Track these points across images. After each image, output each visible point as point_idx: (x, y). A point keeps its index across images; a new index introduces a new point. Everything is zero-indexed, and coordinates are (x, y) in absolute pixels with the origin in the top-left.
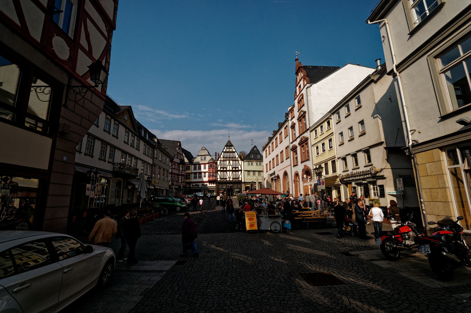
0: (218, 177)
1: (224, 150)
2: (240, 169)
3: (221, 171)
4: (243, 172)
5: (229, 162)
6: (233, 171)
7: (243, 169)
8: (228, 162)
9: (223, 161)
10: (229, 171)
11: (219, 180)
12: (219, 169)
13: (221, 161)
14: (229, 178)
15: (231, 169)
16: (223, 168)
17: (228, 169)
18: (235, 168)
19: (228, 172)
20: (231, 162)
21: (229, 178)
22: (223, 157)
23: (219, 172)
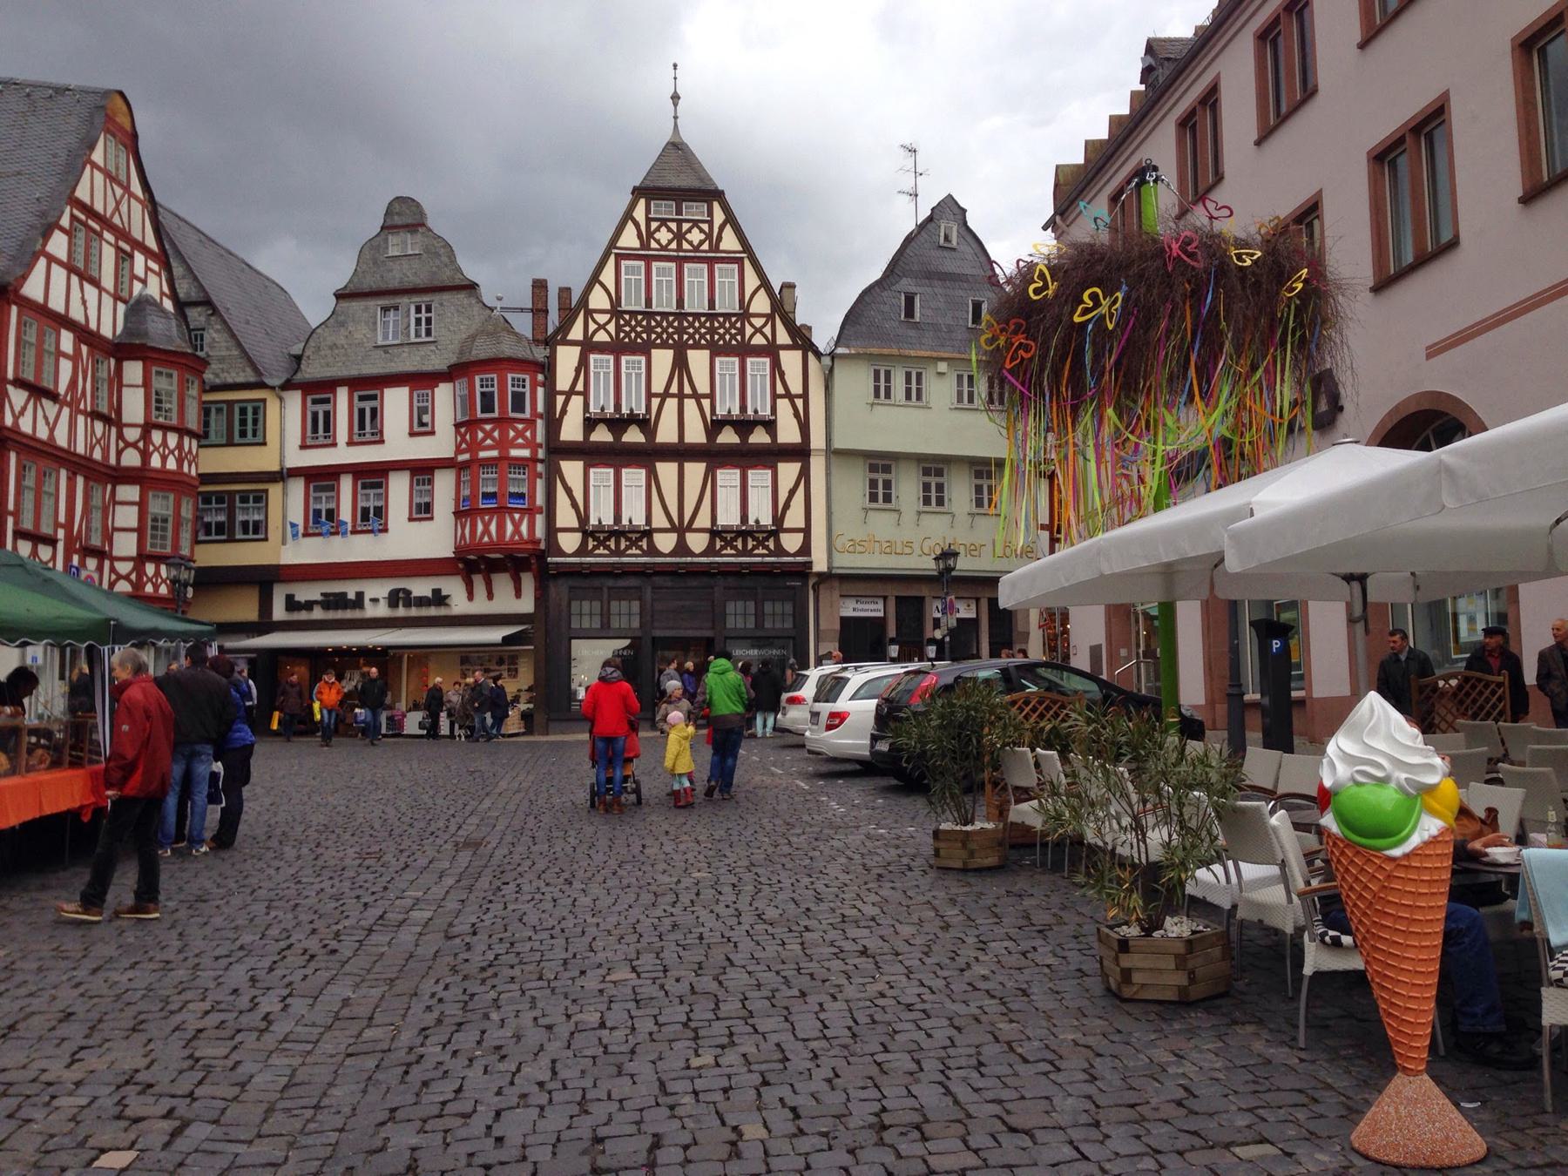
0: (565, 516)
2: (788, 433)
3: (589, 454)
4: (817, 465)
5: (681, 364)
6: (714, 456)
7: (817, 441)
8: (663, 359)
9: (617, 348)
10: (681, 453)
11: (569, 542)
12: (571, 431)
13: (588, 346)
14: (681, 529)
15: (696, 434)
16: (618, 424)
17: (666, 433)
18: (744, 426)
19: (667, 471)
20: (698, 360)
21: (681, 529)
22: (615, 312)
23: (572, 470)
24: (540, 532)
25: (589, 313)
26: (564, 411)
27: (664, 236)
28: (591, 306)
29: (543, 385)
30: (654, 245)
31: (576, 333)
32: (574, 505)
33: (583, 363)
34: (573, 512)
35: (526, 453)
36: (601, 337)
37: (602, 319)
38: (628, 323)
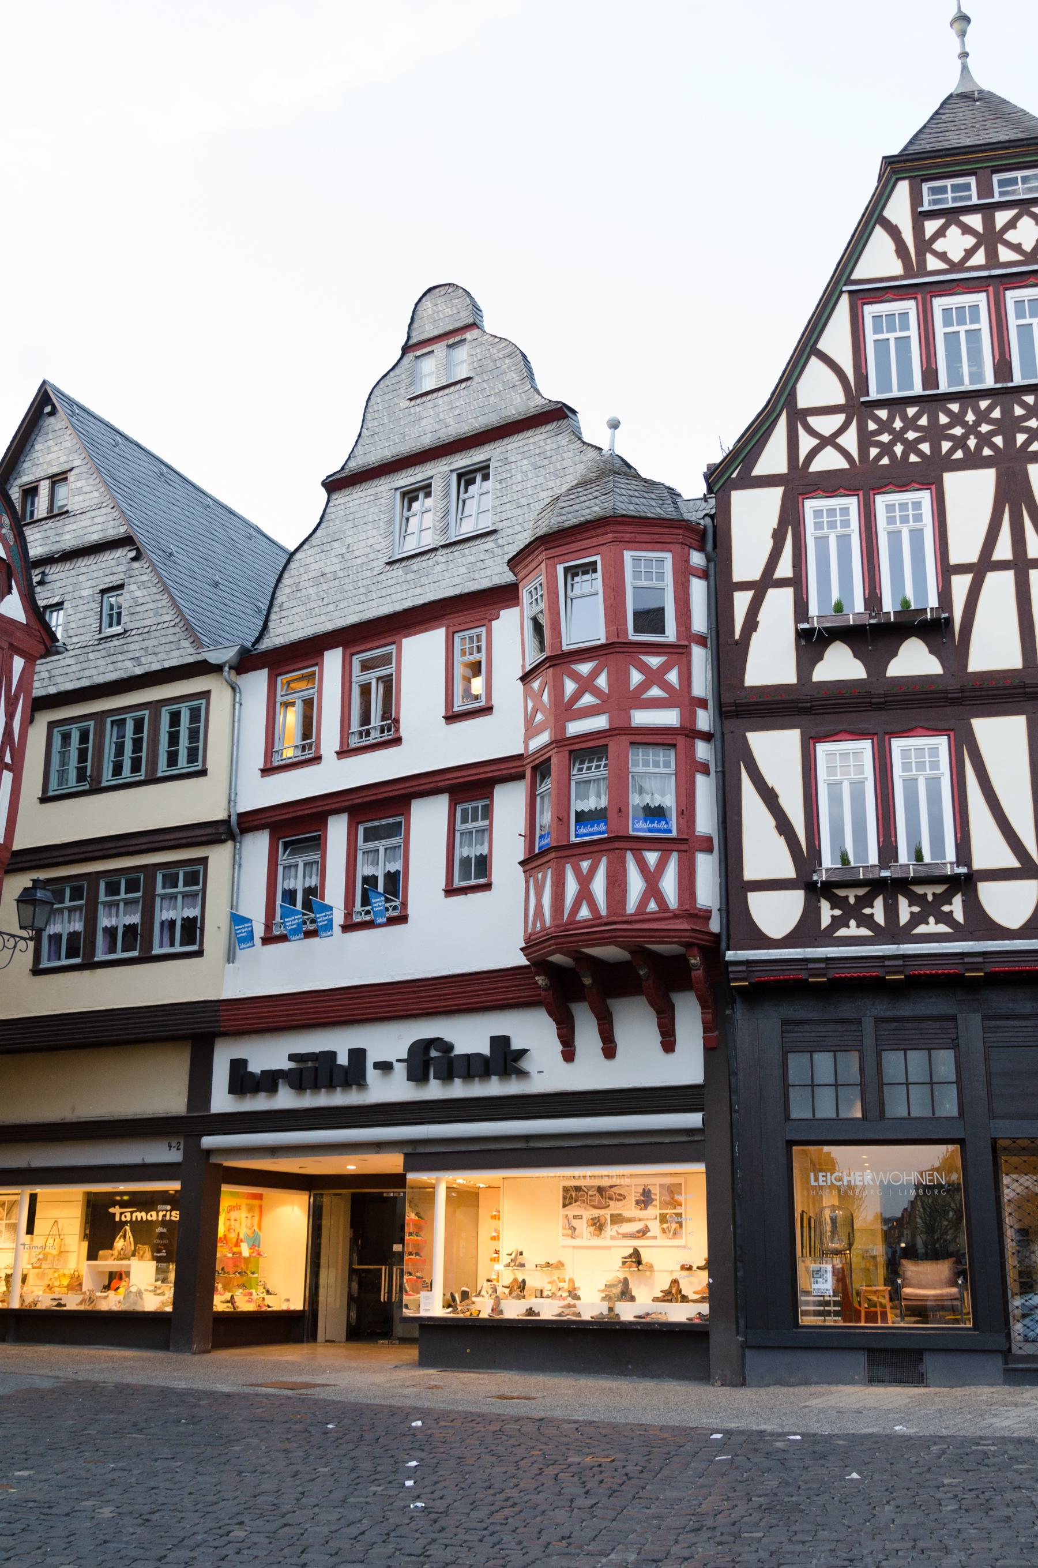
1: (880, 261)
13: (799, 484)
22: (857, 406)
24: (707, 893)
25: (799, 417)
26: (751, 623)
27: (955, 243)
28: (803, 401)
29: (704, 575)
30: (933, 263)
31: (773, 459)
32: (784, 826)
33: (790, 519)
34: (781, 842)
35: (669, 718)
36: (829, 461)
37: (826, 425)
38: (885, 426)
